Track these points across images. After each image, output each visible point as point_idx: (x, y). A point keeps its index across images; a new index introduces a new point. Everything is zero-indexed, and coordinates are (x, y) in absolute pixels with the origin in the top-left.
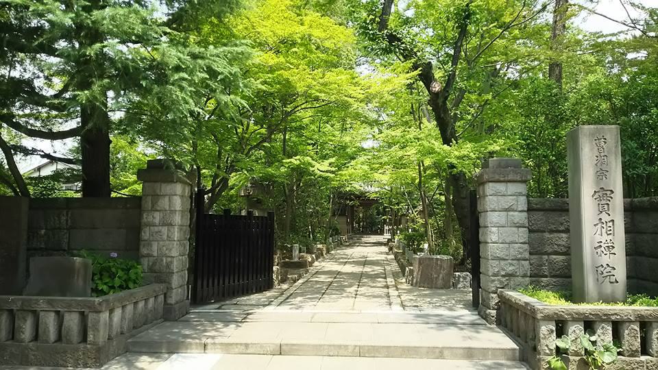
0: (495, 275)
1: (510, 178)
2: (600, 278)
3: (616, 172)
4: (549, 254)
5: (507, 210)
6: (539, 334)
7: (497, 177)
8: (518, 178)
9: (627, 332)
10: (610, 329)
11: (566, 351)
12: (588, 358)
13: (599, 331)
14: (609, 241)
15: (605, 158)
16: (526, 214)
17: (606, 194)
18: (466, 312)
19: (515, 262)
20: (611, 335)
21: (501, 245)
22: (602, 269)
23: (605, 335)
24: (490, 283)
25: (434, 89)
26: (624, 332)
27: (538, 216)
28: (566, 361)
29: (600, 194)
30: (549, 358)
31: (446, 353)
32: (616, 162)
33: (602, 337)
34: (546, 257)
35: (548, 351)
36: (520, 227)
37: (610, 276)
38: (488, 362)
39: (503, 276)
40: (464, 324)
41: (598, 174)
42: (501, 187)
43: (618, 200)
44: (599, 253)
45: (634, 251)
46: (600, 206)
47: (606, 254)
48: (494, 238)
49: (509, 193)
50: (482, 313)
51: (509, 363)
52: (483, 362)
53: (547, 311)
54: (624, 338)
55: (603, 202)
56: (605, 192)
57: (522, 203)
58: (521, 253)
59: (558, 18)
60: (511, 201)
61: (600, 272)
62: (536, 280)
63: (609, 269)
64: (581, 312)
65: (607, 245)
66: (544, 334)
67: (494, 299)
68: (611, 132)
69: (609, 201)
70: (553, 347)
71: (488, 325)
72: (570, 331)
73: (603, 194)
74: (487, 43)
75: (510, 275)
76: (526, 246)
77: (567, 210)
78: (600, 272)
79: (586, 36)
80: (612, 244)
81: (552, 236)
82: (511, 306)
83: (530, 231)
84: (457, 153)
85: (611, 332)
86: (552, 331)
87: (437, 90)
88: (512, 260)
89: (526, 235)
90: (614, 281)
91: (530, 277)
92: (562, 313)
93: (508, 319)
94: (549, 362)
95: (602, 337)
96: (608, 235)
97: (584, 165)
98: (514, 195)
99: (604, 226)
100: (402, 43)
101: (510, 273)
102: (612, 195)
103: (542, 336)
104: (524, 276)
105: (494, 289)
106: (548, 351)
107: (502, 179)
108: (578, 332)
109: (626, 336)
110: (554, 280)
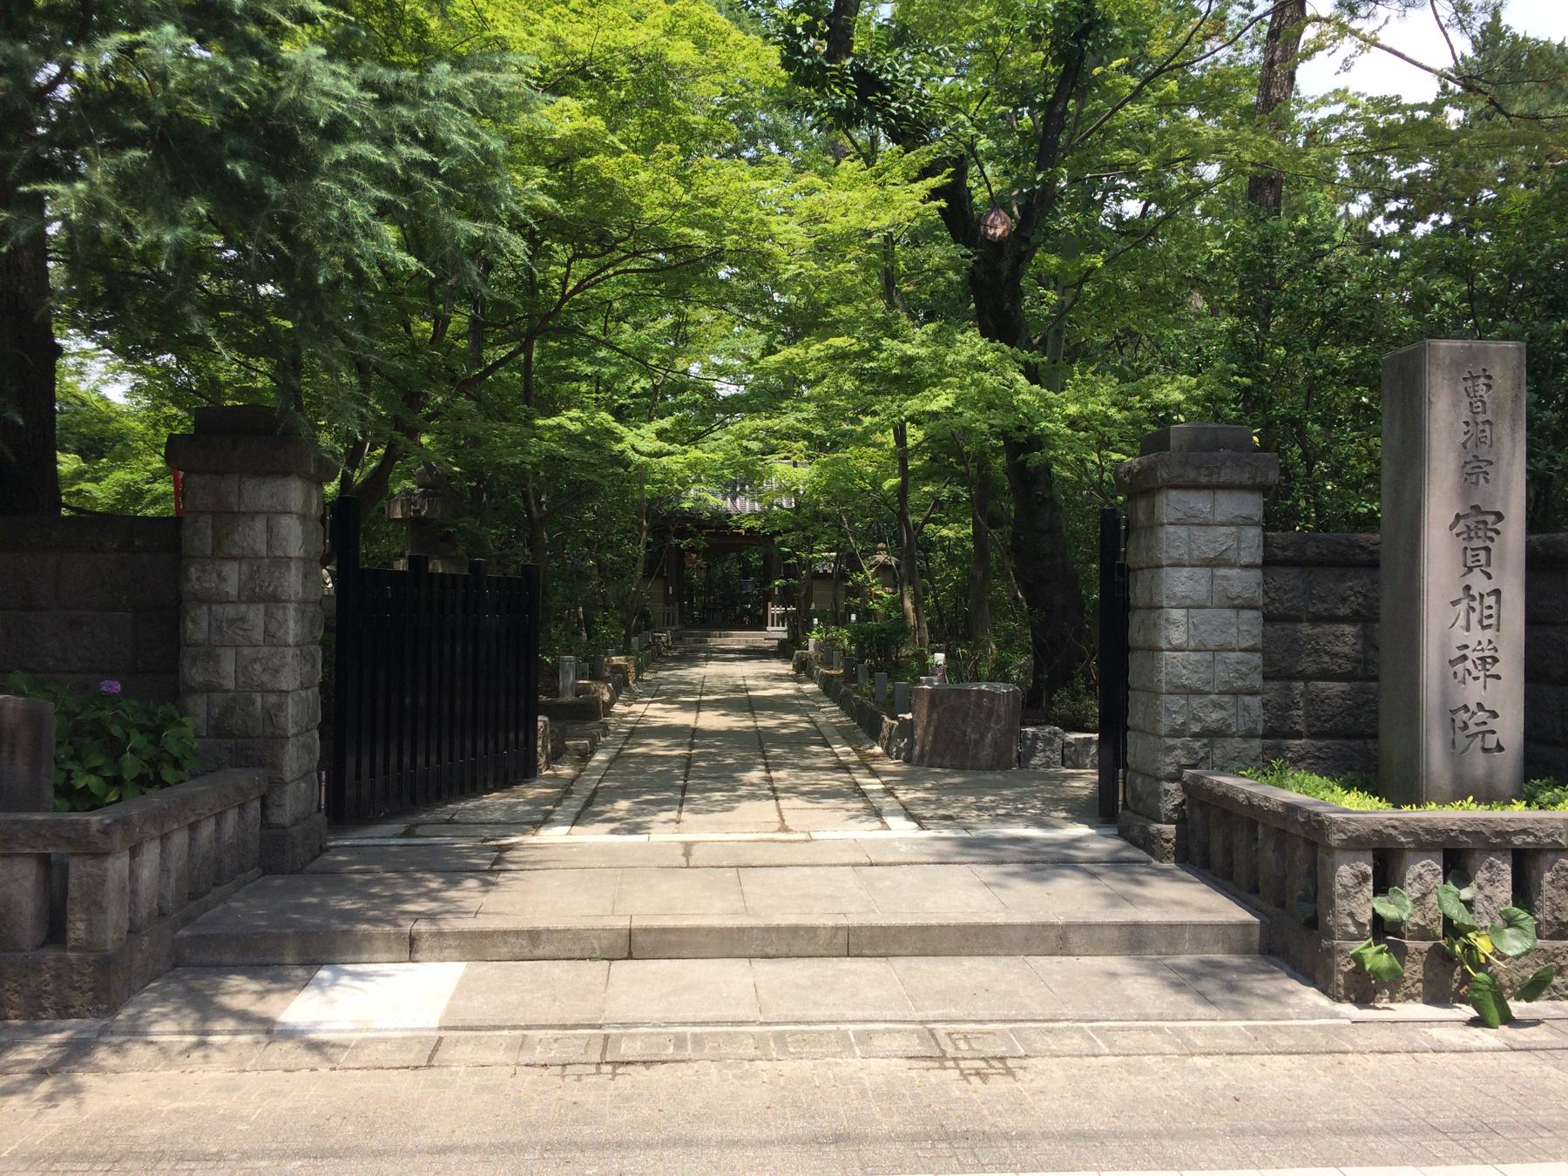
0: (1176, 733)
1: (1226, 476)
2: (1460, 735)
3: (1510, 464)
4: (1307, 678)
5: (1212, 563)
6: (1331, 886)
7: (1191, 475)
8: (1245, 478)
9: (1548, 876)
10: (1507, 867)
11: (1395, 927)
12: (1452, 945)
13: (1481, 876)
14: (1485, 644)
15: (1487, 427)
16: (1258, 573)
17: (1485, 523)
18: (1081, 830)
19: (1226, 698)
20: (1508, 886)
21: (1194, 657)
22: (1466, 716)
23: (1494, 885)
24: (1164, 758)
25: (991, 232)
26: (1541, 877)
27: (1288, 578)
28: (1399, 951)
29: (1471, 522)
30: (1358, 947)
31: (1075, 938)
32: (1513, 439)
33: (1488, 890)
34: (1300, 685)
35: (1352, 929)
36: (1243, 608)
37: (1484, 733)
38: (1184, 960)
39: (1196, 736)
40: (1093, 861)
41: (1468, 469)
42: (1199, 503)
43: (1514, 534)
44: (1460, 676)
45: (1539, 672)
46: (1469, 552)
47: (1476, 678)
48: (1177, 636)
49: (1219, 518)
50: (1135, 832)
51: (1236, 960)
52: (1171, 960)
53: (1354, 826)
54: (1540, 892)
55: (1478, 543)
56: (1480, 518)
57: (1251, 543)
58: (1243, 676)
59: (1278, 53)
60: (1222, 539)
61: (1459, 724)
62: (1274, 745)
63: (1481, 716)
64: (1441, 826)
65: (1481, 654)
66: (1344, 886)
67: (1173, 795)
68: (1504, 359)
69: (1492, 539)
70: (1365, 917)
71: (1156, 863)
72: (1409, 876)
73: (1477, 523)
74: (1096, 113)
75: (1213, 734)
76: (1257, 658)
77: (1374, 565)
78: (1459, 724)
79: (1354, 106)
80: (1492, 653)
81: (1317, 630)
82: (1227, 814)
83: (1269, 619)
84: (1072, 409)
85: (1509, 877)
86: (1365, 878)
87: (999, 232)
88: (1220, 693)
89: (1257, 631)
90: (1493, 745)
91: (1264, 737)
92: (1394, 832)
93: (1217, 845)
94: (1358, 958)
95: (1488, 890)
96: (1484, 628)
97: (1434, 444)
98: (1232, 524)
99: (1476, 604)
100: (895, 98)
101: (1215, 726)
102: (1498, 526)
103: (1339, 889)
104: (1249, 735)
105: (1171, 769)
106: (1352, 929)
107: (1204, 480)
108: (1428, 877)
109: (1545, 886)
110: (1320, 744)
